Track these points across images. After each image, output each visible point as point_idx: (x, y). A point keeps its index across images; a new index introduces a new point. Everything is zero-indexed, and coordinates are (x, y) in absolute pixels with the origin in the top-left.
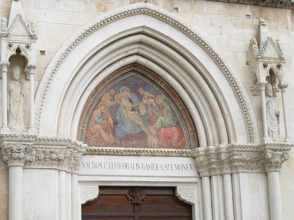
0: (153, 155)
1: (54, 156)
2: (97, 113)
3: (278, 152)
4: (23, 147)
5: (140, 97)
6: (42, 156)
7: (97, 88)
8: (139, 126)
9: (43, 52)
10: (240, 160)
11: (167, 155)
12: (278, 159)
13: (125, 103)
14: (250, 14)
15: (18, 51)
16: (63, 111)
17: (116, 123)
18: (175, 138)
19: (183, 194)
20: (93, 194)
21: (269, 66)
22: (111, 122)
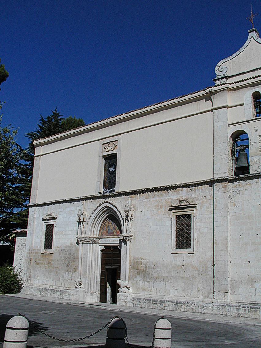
7: (104, 221)
13: (111, 224)
17: (108, 230)
20: (103, 248)
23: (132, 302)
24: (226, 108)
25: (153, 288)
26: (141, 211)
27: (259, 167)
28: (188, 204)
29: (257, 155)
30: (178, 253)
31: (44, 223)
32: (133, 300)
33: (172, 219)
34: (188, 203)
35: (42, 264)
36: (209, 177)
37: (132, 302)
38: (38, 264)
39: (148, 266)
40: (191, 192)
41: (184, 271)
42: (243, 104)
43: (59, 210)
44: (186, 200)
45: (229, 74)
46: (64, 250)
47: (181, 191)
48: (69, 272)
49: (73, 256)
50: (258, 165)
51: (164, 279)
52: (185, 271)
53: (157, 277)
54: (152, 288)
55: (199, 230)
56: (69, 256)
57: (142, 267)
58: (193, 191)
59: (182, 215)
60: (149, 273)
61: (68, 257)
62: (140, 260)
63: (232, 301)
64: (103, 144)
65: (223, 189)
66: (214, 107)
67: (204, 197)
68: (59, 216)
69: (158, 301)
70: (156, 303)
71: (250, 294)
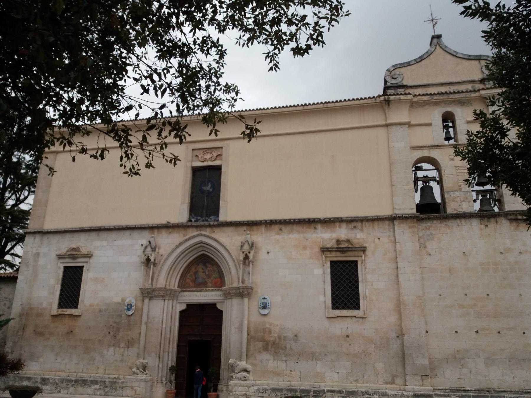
0: (207, 291)
1: (160, 294)
2: (189, 275)
3: (245, 290)
4: (146, 292)
5: (207, 267)
6: (156, 295)
8: (204, 279)
9: (162, 255)
10: (232, 293)
11: (212, 291)
12: (246, 293)
13: (201, 270)
14: (245, 229)
15: (148, 257)
16: (169, 276)
17: (196, 278)
18: (219, 283)
19: (219, 306)
20: (184, 307)
21: (245, 253)
22: (194, 278)
23: (260, 394)
24: (407, 126)
25: (294, 371)
26: (268, 253)
27: (460, 206)
28: (350, 246)
29: (457, 191)
30: (338, 317)
31: (61, 263)
32: (263, 392)
33: (325, 265)
34: (352, 244)
35: (51, 334)
36: (386, 212)
37: (260, 394)
38: (41, 334)
39: (284, 337)
40: (356, 231)
41: (350, 345)
42: (430, 125)
43: (98, 243)
44: (348, 241)
45: (405, 83)
46: (106, 310)
47: (338, 228)
48: (117, 349)
49: (126, 321)
50: (459, 204)
51: (313, 357)
52: (352, 345)
53: (300, 354)
54: (291, 371)
55: (372, 285)
56: (117, 320)
57: (271, 337)
58: (359, 230)
59: (341, 262)
60: (286, 347)
61: (115, 322)
62: (268, 326)
63: (436, 388)
64: (193, 150)
65: (411, 230)
66: (389, 122)
67: (377, 239)
68: (97, 253)
69: (312, 393)
70: (308, 395)
71: (462, 377)
